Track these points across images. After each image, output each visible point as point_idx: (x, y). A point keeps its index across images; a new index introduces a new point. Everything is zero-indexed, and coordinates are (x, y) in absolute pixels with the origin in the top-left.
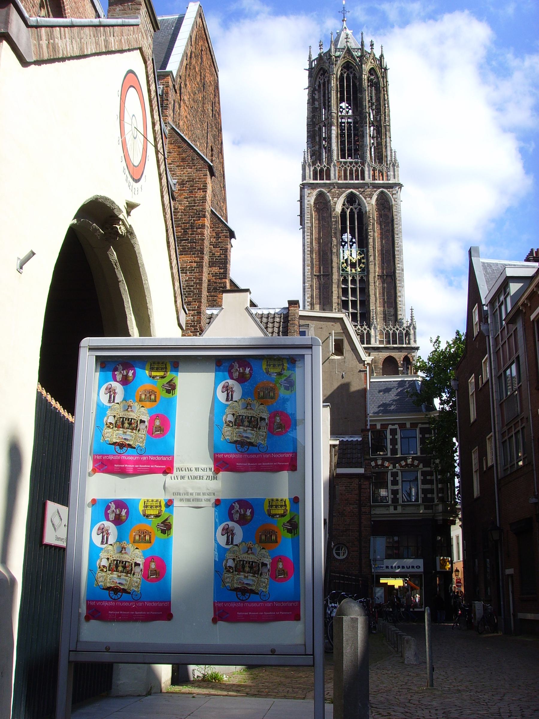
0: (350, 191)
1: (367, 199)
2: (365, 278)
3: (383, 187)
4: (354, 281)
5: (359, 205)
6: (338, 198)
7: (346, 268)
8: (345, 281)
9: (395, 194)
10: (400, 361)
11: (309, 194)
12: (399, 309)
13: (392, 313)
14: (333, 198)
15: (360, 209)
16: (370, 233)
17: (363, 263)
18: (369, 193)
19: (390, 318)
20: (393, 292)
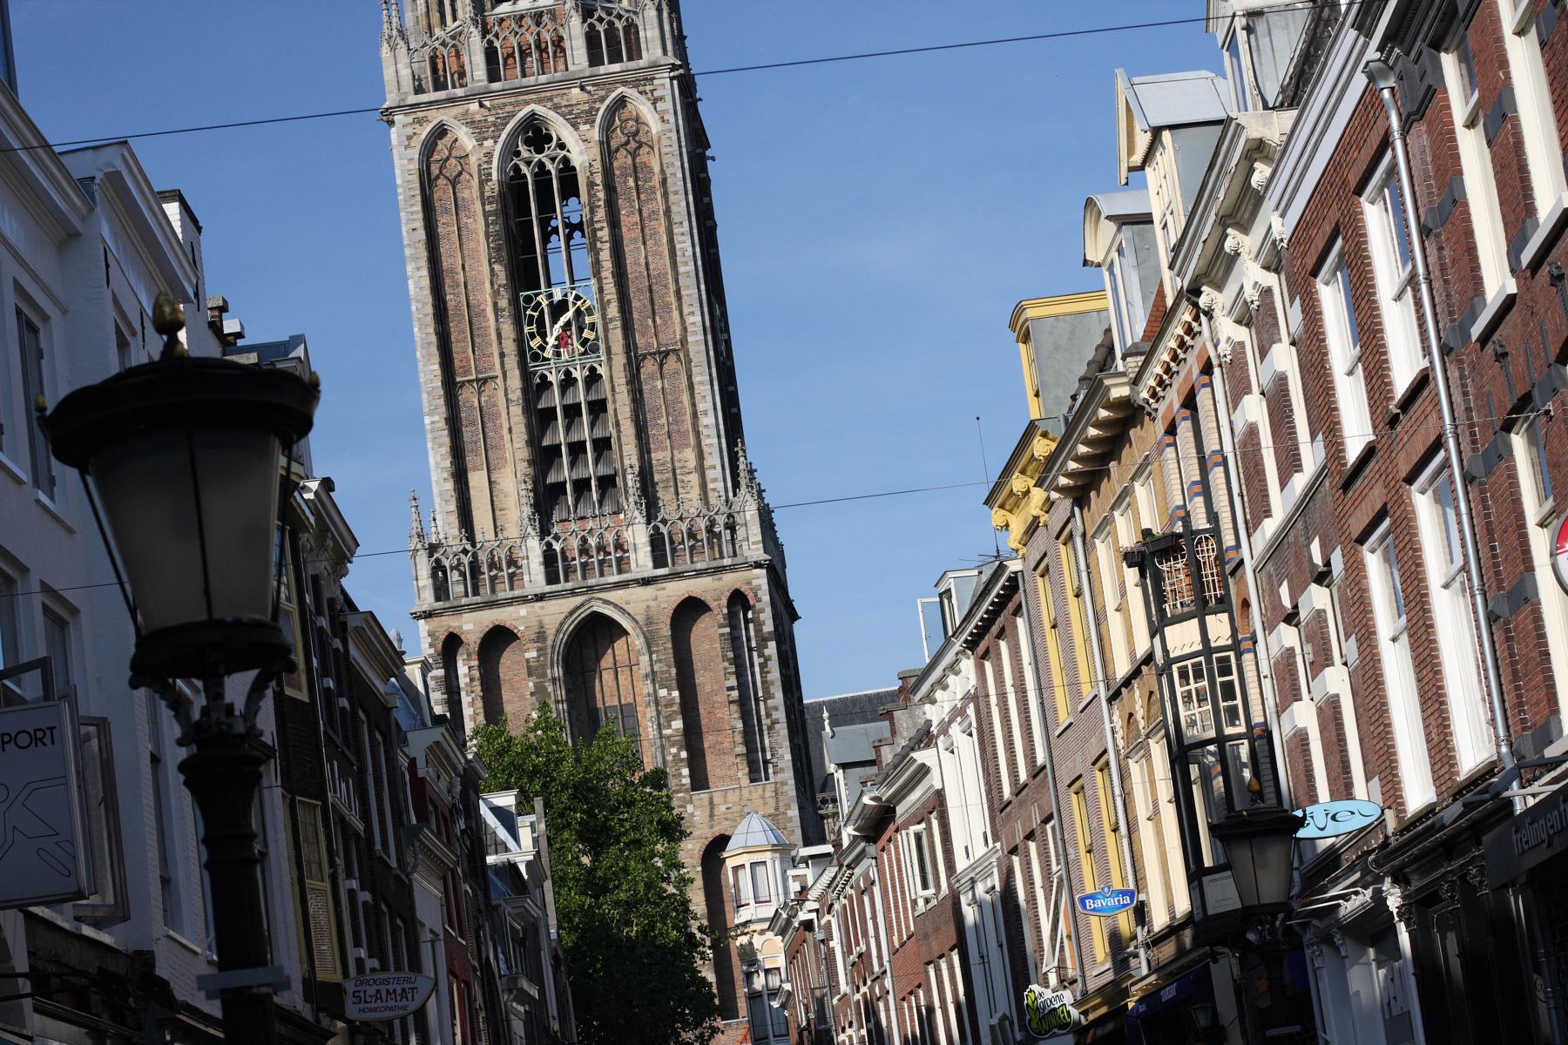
0: (526, 110)
1: (583, 128)
2: (602, 370)
3: (624, 83)
4: (568, 382)
5: (562, 146)
6: (496, 139)
7: (542, 348)
8: (545, 384)
9: (661, 98)
10: (720, 607)
11: (409, 138)
12: (705, 449)
13: (692, 462)
14: (481, 140)
15: (566, 161)
16: (599, 234)
17: (592, 327)
18: (586, 107)
19: (686, 478)
20: (685, 398)
